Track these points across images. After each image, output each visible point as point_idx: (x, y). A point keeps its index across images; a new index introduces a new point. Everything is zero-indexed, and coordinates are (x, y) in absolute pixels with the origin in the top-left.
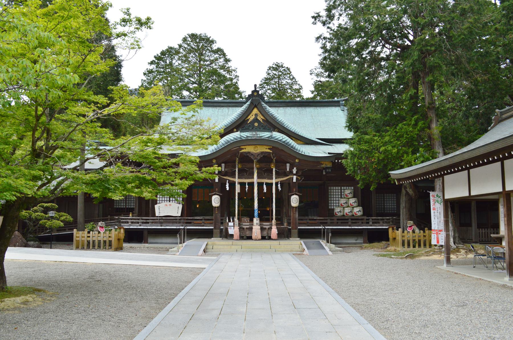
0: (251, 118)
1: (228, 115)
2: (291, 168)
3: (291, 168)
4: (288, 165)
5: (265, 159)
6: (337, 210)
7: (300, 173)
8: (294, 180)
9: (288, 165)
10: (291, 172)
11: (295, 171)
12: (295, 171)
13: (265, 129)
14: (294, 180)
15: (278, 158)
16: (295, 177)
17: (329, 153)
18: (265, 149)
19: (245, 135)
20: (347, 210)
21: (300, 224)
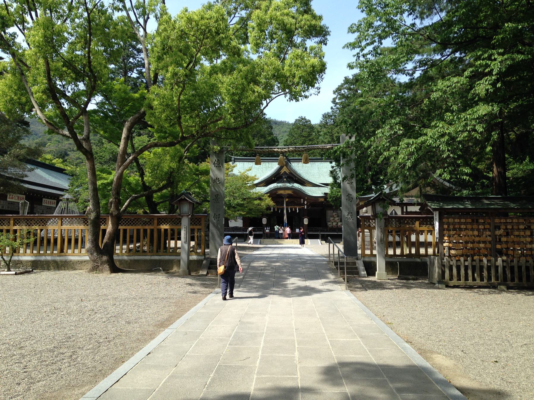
0: (282, 171)
1: (269, 167)
2: (304, 201)
3: (304, 201)
4: (302, 200)
5: (289, 196)
6: (329, 223)
7: (309, 204)
8: (306, 208)
9: (302, 200)
10: (304, 204)
11: (306, 203)
12: (306, 203)
13: (289, 183)
14: (306, 208)
15: (297, 197)
16: (306, 206)
17: (325, 194)
18: (289, 192)
19: (280, 185)
20: (334, 224)
21: (309, 231)
